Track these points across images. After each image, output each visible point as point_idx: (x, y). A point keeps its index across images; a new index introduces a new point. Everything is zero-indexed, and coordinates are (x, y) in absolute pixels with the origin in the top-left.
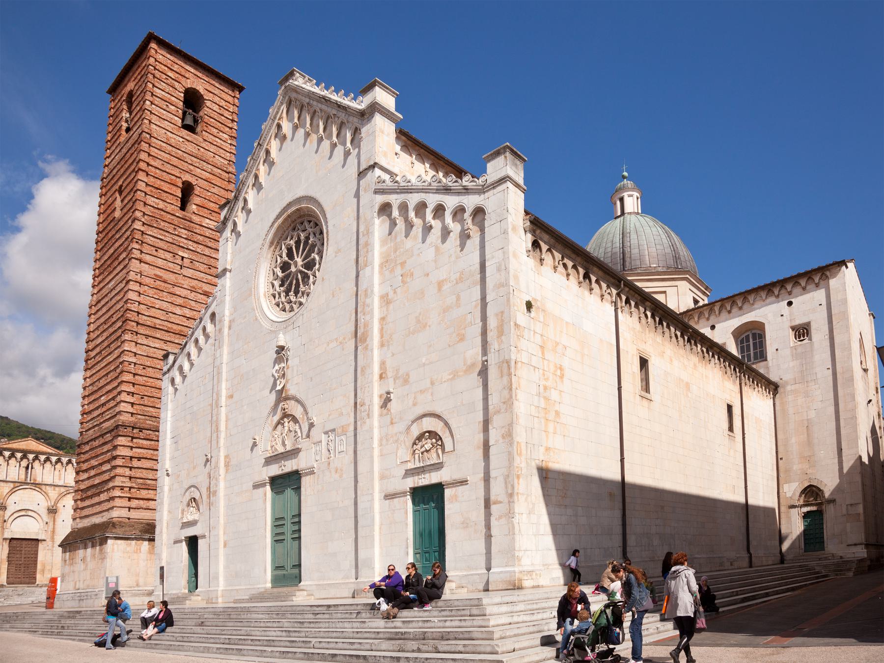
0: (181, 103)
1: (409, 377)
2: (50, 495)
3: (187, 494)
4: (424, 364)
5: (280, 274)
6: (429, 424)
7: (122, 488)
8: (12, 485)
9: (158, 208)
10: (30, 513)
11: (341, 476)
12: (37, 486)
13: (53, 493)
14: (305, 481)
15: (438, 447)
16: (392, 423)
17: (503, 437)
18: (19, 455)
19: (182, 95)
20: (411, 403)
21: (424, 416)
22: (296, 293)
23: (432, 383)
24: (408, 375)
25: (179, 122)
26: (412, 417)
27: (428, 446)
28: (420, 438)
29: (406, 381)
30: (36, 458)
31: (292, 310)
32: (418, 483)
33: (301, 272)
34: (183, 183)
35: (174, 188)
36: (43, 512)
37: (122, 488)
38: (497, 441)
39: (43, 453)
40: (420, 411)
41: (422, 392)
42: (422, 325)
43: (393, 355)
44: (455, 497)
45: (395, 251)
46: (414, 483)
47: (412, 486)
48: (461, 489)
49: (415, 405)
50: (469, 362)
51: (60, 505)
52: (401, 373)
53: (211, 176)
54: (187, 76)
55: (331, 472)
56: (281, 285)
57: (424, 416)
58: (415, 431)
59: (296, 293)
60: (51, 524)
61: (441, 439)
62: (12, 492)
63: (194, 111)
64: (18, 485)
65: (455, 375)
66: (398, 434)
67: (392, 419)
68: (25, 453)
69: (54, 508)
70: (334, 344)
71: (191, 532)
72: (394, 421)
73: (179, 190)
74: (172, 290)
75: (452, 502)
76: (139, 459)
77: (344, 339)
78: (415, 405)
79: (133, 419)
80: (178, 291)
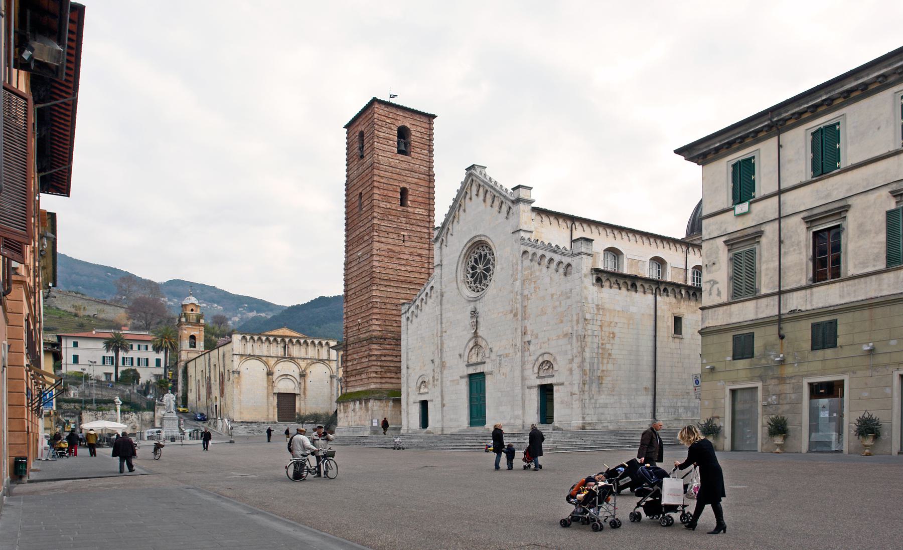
0: (396, 138)
2: (301, 365)
3: (420, 379)
5: (471, 272)
6: (546, 357)
7: (376, 372)
8: (276, 359)
9: (387, 208)
10: (289, 377)
11: (506, 377)
12: (292, 359)
13: (303, 364)
14: (488, 379)
16: (530, 355)
17: (578, 367)
18: (279, 339)
19: (396, 132)
21: (545, 353)
22: (480, 283)
23: (549, 340)
24: (537, 334)
25: (396, 150)
26: (540, 354)
27: (547, 367)
28: (543, 363)
29: (537, 337)
30: (291, 341)
31: (478, 292)
33: (483, 273)
34: (401, 189)
35: (396, 193)
36: (297, 375)
37: (376, 372)
39: (295, 337)
40: (543, 351)
41: (544, 343)
42: (543, 312)
43: (530, 324)
44: (558, 390)
45: (531, 275)
48: (561, 387)
49: (540, 348)
50: (565, 333)
51: (308, 371)
52: (534, 333)
53: (418, 181)
54: (398, 119)
56: (472, 277)
57: (545, 353)
58: (541, 360)
59: (480, 283)
60: (303, 384)
62: (276, 363)
63: (404, 139)
64: (280, 359)
65: (558, 337)
68: (283, 338)
69: (304, 373)
70: (501, 314)
71: (423, 398)
73: (399, 194)
74: (399, 256)
76: (385, 356)
78: (540, 348)
79: (380, 334)
80: (402, 256)
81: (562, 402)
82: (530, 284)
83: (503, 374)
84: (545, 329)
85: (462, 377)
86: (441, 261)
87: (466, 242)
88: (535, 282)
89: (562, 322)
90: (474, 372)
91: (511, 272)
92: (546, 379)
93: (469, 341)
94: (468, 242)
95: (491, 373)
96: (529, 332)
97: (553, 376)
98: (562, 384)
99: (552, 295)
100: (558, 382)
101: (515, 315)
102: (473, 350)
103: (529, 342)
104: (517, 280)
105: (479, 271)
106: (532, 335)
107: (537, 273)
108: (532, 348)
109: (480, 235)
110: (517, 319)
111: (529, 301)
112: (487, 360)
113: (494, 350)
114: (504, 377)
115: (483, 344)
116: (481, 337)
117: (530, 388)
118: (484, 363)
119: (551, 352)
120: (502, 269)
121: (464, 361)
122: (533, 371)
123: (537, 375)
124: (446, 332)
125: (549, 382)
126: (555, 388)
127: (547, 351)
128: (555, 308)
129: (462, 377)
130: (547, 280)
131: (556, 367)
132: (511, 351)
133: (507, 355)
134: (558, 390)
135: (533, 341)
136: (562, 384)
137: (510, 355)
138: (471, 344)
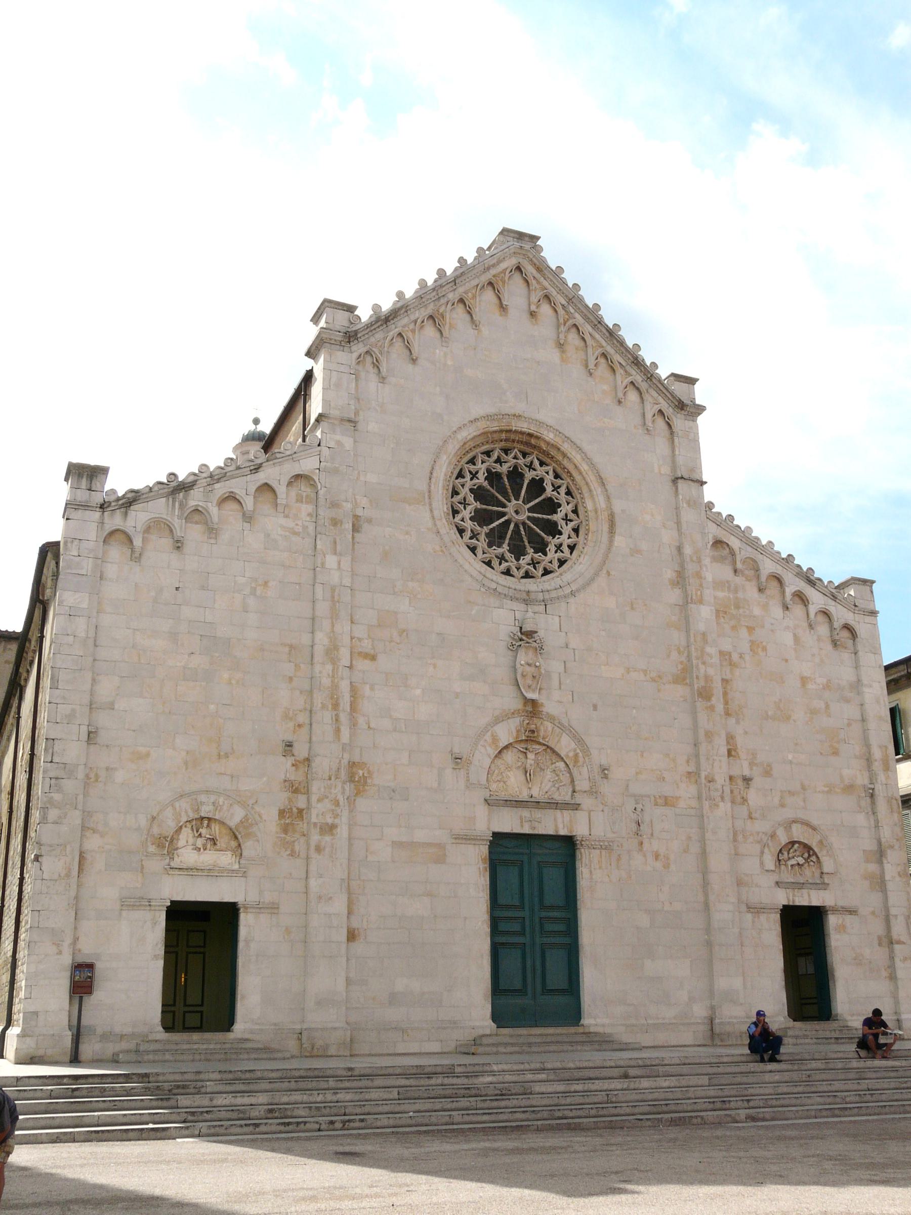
1: (771, 769)
4: (791, 762)
6: (798, 833)
11: (667, 866)
15: (812, 863)
20: (776, 800)
23: (804, 788)
29: (768, 772)
32: (793, 901)
38: (893, 877)
40: (789, 814)
43: (746, 733)
44: (842, 928)
46: (789, 900)
47: (786, 903)
48: (848, 918)
49: (782, 805)
55: (645, 856)
59: (518, 552)
61: (815, 854)
65: (830, 790)
66: (761, 834)
67: (750, 813)
72: (754, 815)
75: (840, 932)
77: (659, 677)
81: (858, 961)
82: (734, 628)
83: (657, 857)
84: (790, 757)
85: (463, 839)
86: (357, 413)
87: (478, 411)
88: (751, 629)
89: (836, 753)
90: (526, 830)
91: (669, 574)
92: (805, 891)
93: (497, 720)
94: (488, 417)
95: (606, 847)
96: (743, 754)
97: (824, 886)
98: (852, 912)
99: (804, 680)
100: (841, 903)
101: (705, 694)
102: (510, 757)
103: (747, 780)
104: (701, 601)
105: (523, 517)
106: (752, 764)
107: (757, 611)
108: (754, 797)
109: (541, 424)
110: (712, 708)
111: (737, 672)
112: (586, 802)
113: (617, 774)
114: (659, 865)
115: (565, 745)
116: (552, 719)
117: (756, 910)
118: (576, 807)
119: (815, 822)
120: (636, 551)
121: (469, 785)
122: (762, 863)
123: (775, 877)
124: (373, 658)
125: (815, 903)
126: (832, 921)
127: (801, 815)
128: (814, 712)
129: (463, 839)
130: (788, 638)
131: (828, 865)
132: (686, 792)
133: (667, 802)
134: (842, 928)
135: (758, 781)
136: (852, 912)
137: (682, 804)
138: (506, 733)
